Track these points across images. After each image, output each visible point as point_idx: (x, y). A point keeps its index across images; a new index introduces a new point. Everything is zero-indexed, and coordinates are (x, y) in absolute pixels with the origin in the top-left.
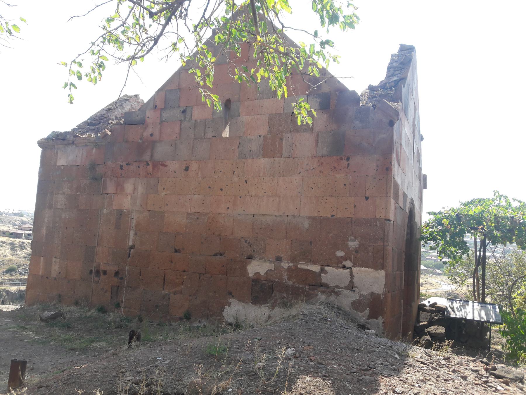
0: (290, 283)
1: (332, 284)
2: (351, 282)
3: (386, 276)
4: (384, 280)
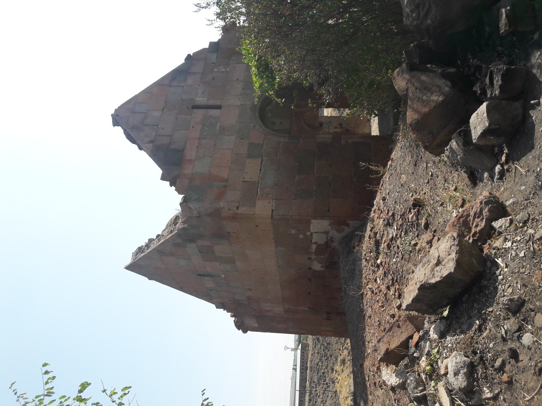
0: (327, 255)
1: (326, 240)
2: (322, 233)
3: (315, 218)
4: (318, 221)
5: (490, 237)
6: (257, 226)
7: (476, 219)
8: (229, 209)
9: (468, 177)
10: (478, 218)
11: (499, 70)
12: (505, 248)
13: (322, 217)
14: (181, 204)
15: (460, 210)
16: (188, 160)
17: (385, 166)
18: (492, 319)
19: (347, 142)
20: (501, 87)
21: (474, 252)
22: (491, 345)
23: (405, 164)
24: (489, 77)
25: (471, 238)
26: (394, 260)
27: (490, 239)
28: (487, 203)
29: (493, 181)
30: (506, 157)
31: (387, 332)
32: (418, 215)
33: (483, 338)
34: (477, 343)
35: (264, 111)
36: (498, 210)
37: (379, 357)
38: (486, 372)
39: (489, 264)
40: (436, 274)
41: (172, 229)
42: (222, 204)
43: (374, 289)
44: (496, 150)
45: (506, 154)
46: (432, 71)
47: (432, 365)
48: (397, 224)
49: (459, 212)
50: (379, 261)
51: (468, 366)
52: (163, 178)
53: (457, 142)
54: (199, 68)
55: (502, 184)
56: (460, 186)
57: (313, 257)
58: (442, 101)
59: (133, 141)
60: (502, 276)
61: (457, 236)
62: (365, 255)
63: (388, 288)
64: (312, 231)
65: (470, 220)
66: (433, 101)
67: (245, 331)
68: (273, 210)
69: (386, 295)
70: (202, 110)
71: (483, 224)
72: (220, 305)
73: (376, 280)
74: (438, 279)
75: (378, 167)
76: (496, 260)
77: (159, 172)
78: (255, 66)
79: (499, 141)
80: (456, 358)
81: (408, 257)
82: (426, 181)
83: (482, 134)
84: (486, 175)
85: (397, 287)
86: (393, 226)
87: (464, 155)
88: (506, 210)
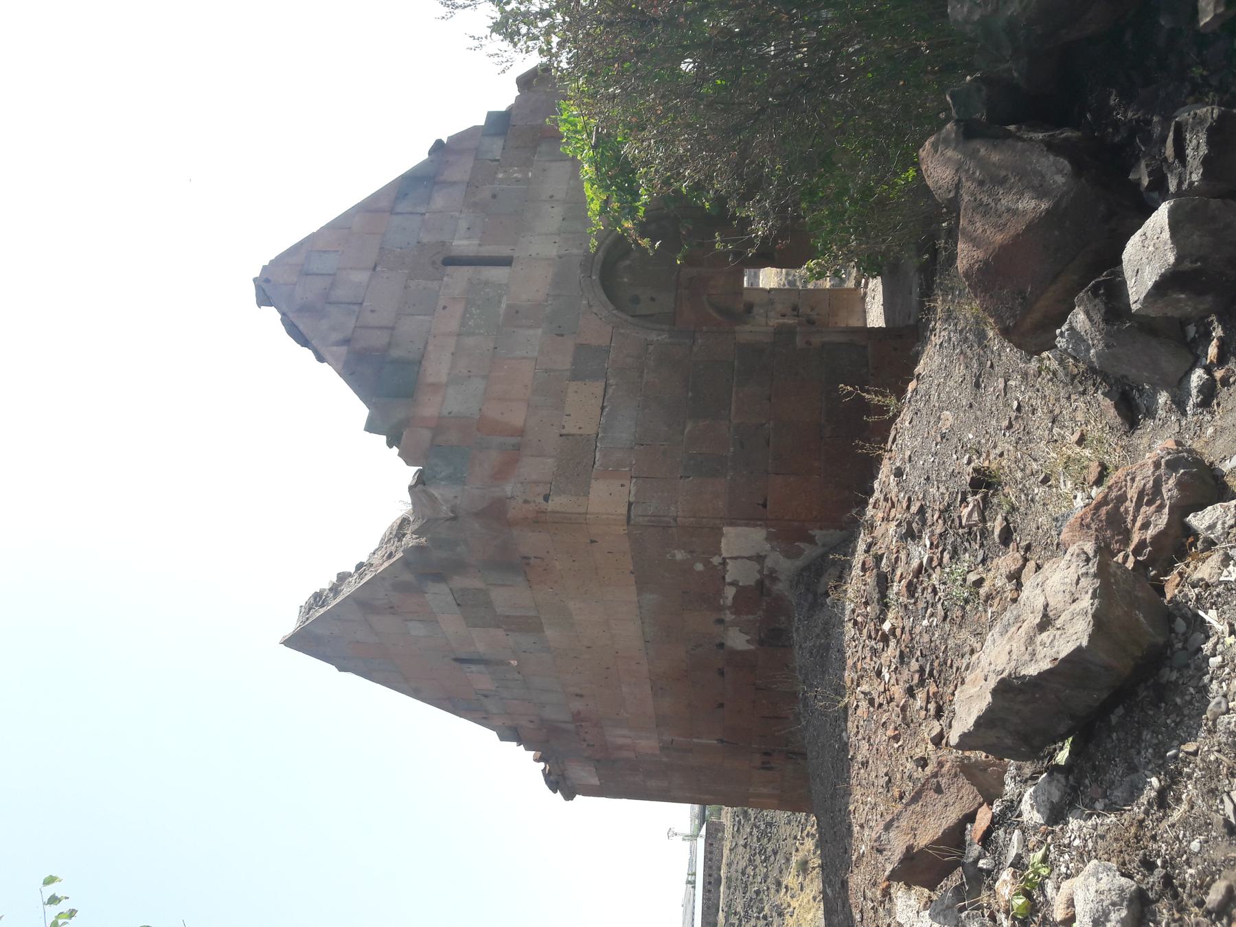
0: (761, 613)
1: (758, 577)
2: (749, 558)
3: (731, 524)
4: (739, 529)
5: (1181, 553)
6: (592, 541)
7: (1144, 509)
8: (526, 502)
9: (1116, 406)
10: (1149, 503)
11: (1202, 121)
12: (1226, 583)
13: (750, 520)
14: (411, 488)
15: (1095, 492)
16: (433, 385)
17: (900, 393)
18: (1198, 774)
19: (808, 343)
20: (1206, 162)
21: (1140, 594)
22: (1195, 846)
23: (952, 383)
24: (1175, 140)
25: (1131, 559)
26: (925, 623)
27: (1181, 559)
28: (1172, 465)
29: (1184, 413)
30: (1220, 348)
31: (908, 805)
32: (985, 508)
33: (1173, 826)
34: (1154, 838)
35: (612, 268)
36: (1205, 484)
37: (889, 868)
38: (1181, 919)
39: (1180, 625)
40: (1041, 652)
41: (393, 549)
42: (509, 489)
43: (875, 695)
44: (1192, 331)
45: (1220, 339)
46: (1020, 139)
47: (1028, 894)
48: (932, 532)
49: (1089, 497)
50: (886, 626)
51: (1131, 901)
52: (371, 427)
53: (1087, 313)
54: (461, 171)
55: (1208, 417)
56: (1093, 432)
57: (729, 617)
58: (1048, 211)
59: (303, 341)
60: (1219, 659)
61: (1096, 552)
62: (853, 611)
63: (910, 692)
64: (725, 555)
65: (1127, 512)
66: (1025, 212)
67: (569, 796)
68: (630, 504)
69: (904, 709)
70: (466, 268)
71: (1162, 521)
72: (510, 733)
73: (879, 673)
74: (1046, 665)
75: (885, 396)
76: (1201, 613)
77: (362, 412)
78: (592, 161)
79: (1201, 307)
80: (1098, 880)
81: (959, 613)
82: (1006, 423)
83: (1157, 285)
84: (1163, 398)
85: (933, 689)
86: (920, 537)
87: (1107, 346)
88: (1225, 484)
